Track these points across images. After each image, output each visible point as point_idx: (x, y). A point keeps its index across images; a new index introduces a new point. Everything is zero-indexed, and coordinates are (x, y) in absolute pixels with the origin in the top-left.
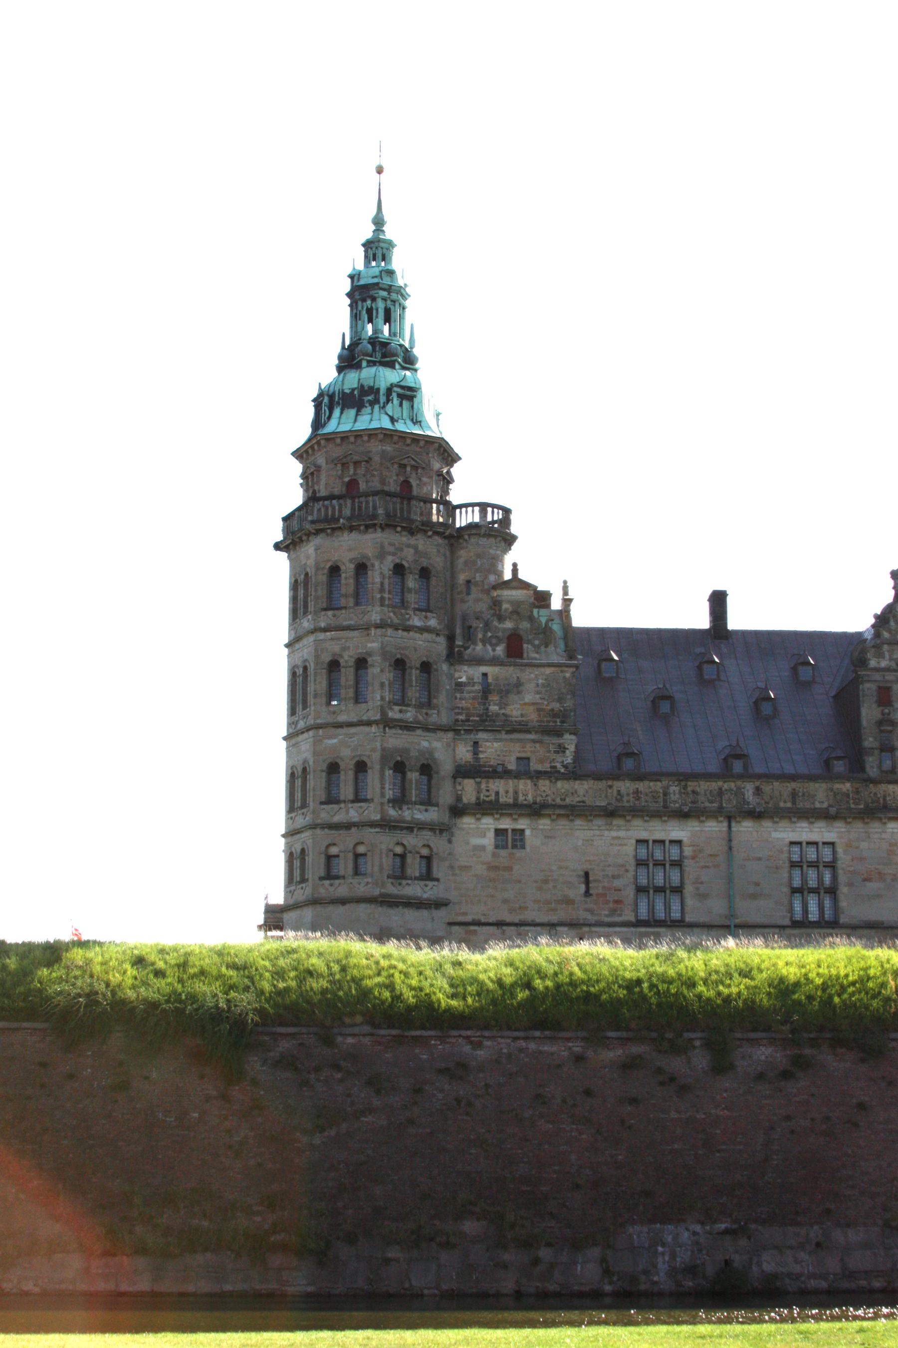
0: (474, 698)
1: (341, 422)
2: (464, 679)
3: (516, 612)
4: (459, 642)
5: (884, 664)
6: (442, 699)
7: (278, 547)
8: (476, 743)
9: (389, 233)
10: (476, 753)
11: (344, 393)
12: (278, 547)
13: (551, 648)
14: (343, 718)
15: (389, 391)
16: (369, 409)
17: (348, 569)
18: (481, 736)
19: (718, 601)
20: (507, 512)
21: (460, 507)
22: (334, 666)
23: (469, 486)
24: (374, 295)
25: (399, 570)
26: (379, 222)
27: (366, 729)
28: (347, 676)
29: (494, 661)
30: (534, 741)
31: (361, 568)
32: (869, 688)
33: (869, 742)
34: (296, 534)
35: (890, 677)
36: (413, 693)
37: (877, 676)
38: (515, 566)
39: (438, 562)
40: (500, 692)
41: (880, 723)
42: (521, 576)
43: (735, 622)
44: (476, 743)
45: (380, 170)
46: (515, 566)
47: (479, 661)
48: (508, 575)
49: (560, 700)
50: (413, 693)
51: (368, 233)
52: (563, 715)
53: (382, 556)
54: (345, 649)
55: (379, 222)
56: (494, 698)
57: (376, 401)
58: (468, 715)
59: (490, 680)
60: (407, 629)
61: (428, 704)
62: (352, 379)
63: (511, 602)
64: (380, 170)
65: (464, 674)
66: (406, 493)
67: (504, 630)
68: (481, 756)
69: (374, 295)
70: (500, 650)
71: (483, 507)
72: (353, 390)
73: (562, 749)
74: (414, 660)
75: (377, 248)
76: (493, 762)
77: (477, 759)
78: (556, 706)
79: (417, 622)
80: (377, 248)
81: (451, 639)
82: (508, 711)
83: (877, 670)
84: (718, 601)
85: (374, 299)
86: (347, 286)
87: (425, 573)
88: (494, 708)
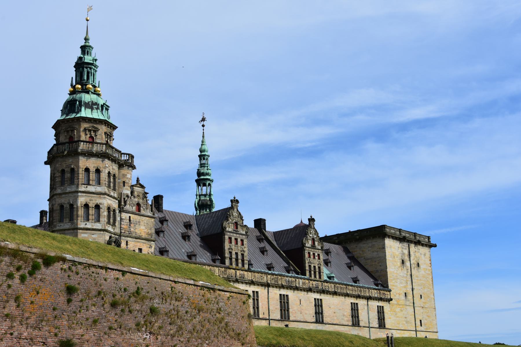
0: (127, 225)
1: (85, 113)
2: (124, 218)
3: (138, 196)
4: (123, 203)
5: (230, 230)
6: (117, 224)
8: (127, 242)
9: (91, 43)
10: (127, 245)
11: (85, 102)
13: (148, 210)
14: (89, 225)
15: (102, 106)
16: (96, 111)
17: (92, 169)
18: (129, 239)
21: (124, 154)
22: (86, 206)
25: (109, 173)
27: (99, 232)
28: (92, 211)
29: (133, 213)
30: (143, 243)
31: (98, 171)
32: (227, 237)
33: (227, 255)
35: (231, 234)
36: (111, 221)
37: (228, 234)
38: (138, 178)
39: (117, 173)
40: (134, 224)
41: (229, 249)
42: (141, 182)
43: (166, 206)
44: (127, 242)
46: (138, 178)
47: (127, 212)
48: (135, 183)
49: (150, 229)
50: (111, 221)
52: (151, 235)
53: (105, 167)
54: (90, 200)
55: (86, 39)
56: (132, 225)
57: (97, 109)
58: (125, 231)
59: (131, 219)
60: (111, 196)
61: (114, 225)
62: (87, 98)
63: (137, 192)
65: (125, 215)
66: (107, 144)
67: (135, 201)
68: (128, 246)
70: (134, 209)
71: (129, 154)
72: (89, 102)
73: (151, 247)
74: (112, 209)
75: (85, 49)
76: (132, 249)
77: (127, 247)
78: (149, 231)
79: (112, 194)
81: (120, 202)
82: (136, 231)
83: (229, 232)
85: (91, 68)
86: (76, 60)
87: (114, 175)
88: (132, 229)
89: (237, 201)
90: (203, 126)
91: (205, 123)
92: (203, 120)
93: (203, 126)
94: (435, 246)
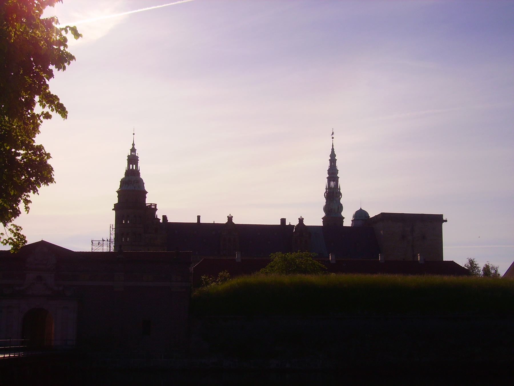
7: (113, 210)
9: (136, 147)
12: (113, 210)
19: (199, 217)
20: (156, 205)
23: (149, 200)
24: (133, 159)
26: (133, 145)
34: (117, 208)
45: (134, 134)
51: (131, 147)
55: (133, 145)
64: (134, 134)
69: (133, 159)
75: (133, 150)
80: (133, 150)
84: (199, 217)
89: (232, 217)
90: (333, 138)
91: (334, 136)
92: (333, 134)
93: (333, 138)
94: (446, 221)
